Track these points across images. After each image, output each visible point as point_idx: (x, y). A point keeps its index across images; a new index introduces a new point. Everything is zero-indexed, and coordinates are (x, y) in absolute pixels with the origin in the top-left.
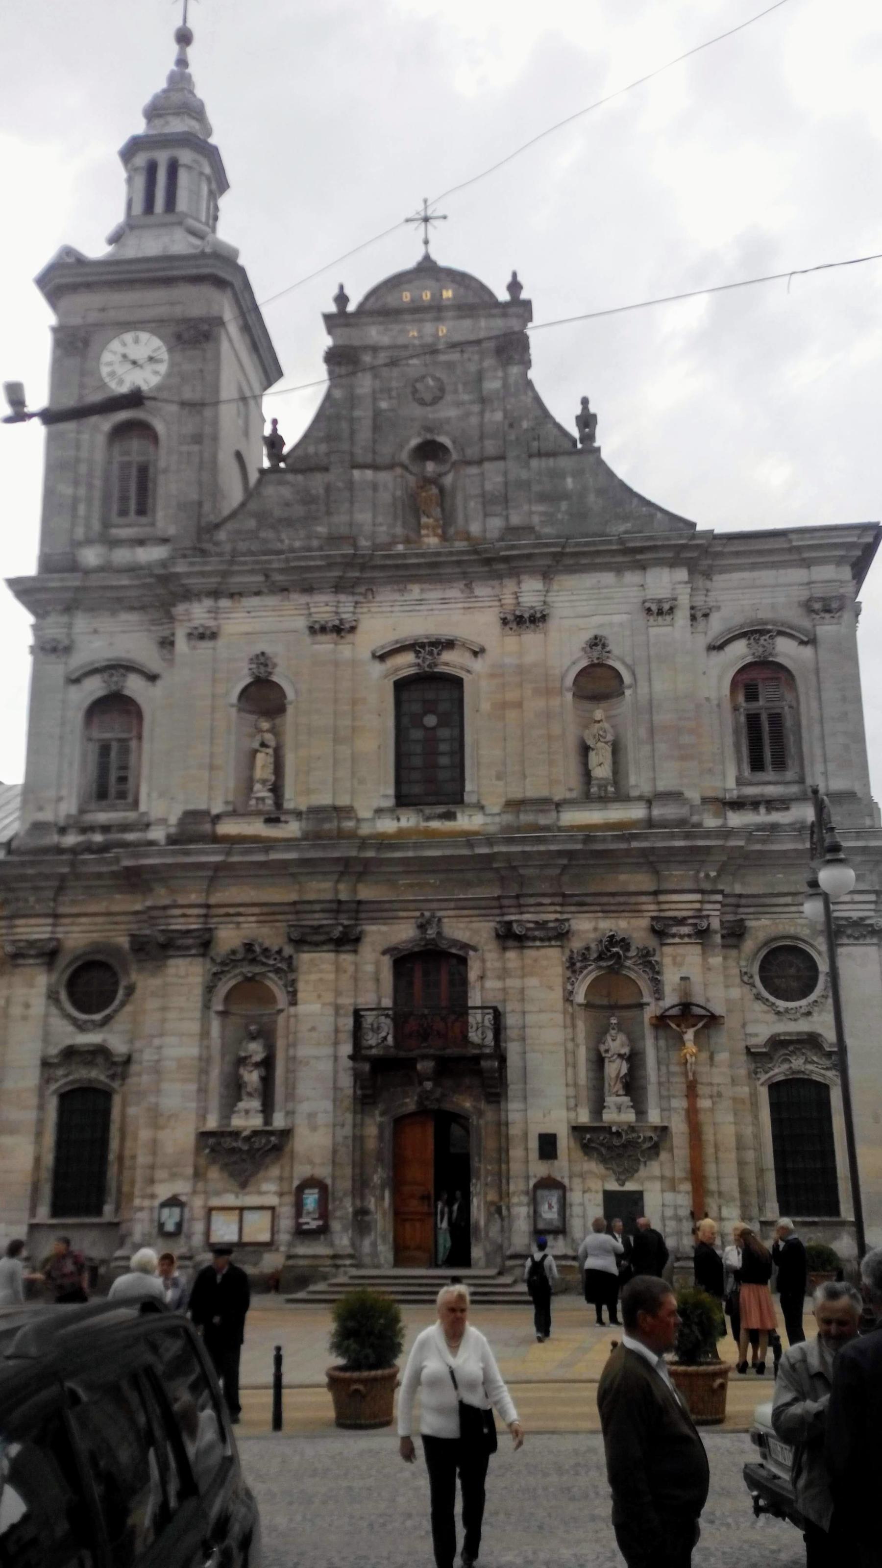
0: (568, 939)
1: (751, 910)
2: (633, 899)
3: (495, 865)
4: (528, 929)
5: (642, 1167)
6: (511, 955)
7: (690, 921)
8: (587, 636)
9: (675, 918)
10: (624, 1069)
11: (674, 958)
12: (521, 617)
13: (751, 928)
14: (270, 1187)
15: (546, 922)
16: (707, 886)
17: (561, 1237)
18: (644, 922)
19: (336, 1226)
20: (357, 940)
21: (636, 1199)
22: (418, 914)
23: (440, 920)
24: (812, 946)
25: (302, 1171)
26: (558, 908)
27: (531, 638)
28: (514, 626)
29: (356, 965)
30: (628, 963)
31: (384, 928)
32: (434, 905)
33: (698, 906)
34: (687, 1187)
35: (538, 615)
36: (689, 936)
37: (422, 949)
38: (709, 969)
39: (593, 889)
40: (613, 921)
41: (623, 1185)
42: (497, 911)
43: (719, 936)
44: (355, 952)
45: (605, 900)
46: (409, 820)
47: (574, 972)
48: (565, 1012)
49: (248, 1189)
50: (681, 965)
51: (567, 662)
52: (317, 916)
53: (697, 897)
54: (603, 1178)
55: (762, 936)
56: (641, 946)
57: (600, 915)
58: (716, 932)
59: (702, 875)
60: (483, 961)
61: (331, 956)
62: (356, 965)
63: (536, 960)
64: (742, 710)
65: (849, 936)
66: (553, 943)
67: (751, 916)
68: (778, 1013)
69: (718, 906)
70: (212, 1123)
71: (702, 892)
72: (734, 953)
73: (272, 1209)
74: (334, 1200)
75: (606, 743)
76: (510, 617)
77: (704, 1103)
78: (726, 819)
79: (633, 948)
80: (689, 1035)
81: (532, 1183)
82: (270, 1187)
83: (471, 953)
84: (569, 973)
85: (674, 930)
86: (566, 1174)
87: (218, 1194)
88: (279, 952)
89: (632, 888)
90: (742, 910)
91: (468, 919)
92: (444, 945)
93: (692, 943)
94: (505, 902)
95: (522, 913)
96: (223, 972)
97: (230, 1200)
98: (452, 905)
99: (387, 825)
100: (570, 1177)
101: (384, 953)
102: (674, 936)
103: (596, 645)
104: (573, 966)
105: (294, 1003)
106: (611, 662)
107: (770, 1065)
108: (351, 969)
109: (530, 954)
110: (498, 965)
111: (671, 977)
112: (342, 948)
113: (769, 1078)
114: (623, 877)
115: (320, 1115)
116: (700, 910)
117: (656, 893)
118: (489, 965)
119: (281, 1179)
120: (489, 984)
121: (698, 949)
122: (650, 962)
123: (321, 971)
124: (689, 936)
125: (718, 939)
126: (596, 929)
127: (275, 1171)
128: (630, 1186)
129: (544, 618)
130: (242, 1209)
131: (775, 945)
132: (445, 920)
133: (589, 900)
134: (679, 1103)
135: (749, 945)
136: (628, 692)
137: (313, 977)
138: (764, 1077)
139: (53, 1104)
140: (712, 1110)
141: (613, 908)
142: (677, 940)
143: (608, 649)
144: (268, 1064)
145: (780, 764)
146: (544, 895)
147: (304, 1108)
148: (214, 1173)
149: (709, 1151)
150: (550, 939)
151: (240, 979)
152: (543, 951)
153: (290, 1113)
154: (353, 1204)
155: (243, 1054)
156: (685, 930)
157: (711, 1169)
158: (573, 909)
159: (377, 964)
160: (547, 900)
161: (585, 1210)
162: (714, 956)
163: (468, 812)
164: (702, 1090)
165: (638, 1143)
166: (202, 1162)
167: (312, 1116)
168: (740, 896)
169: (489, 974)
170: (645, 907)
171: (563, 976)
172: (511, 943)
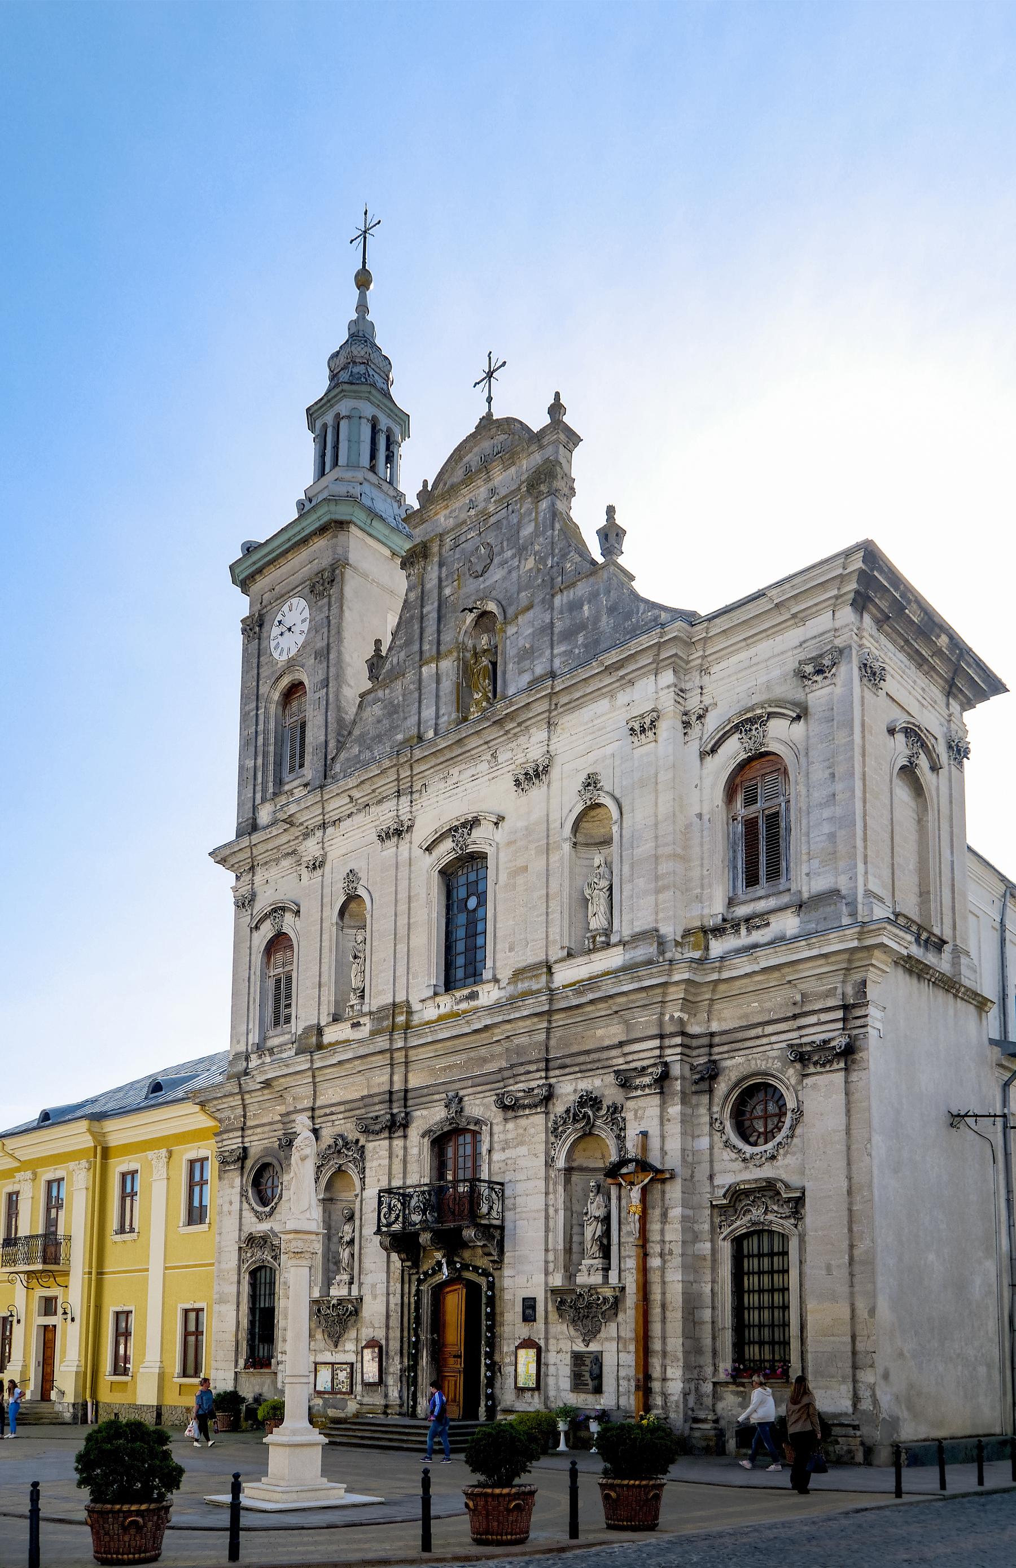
0: (554, 1104)
1: (725, 1048)
2: (605, 1055)
3: (495, 1039)
4: (517, 1099)
5: (603, 1328)
6: (510, 1125)
7: (650, 1070)
8: (582, 777)
9: (636, 1069)
10: (598, 1233)
11: (636, 1111)
12: (526, 774)
13: (724, 1069)
14: (350, 1346)
15: (533, 1089)
16: (669, 1029)
17: (536, 1393)
18: (611, 1079)
19: (391, 1380)
20: (405, 1126)
21: (597, 1359)
22: (444, 1096)
23: (461, 1100)
24: (781, 1080)
25: (367, 1333)
26: (543, 1074)
27: (537, 792)
28: (527, 787)
29: (405, 1148)
30: (599, 1122)
31: (425, 1112)
32: (458, 1085)
33: (657, 1052)
34: (632, 1348)
35: (541, 769)
36: (649, 1086)
37: (450, 1128)
38: (669, 1120)
39: (575, 1049)
40: (590, 1080)
41: (587, 1346)
42: (501, 1084)
43: (679, 1082)
44: (405, 1137)
45: (582, 1059)
46: (446, 1003)
47: (556, 1137)
48: (547, 1178)
49: (340, 1348)
50: (642, 1118)
51: (566, 811)
52: (377, 1108)
53: (656, 1043)
54: (572, 1339)
55: (734, 1076)
56: (610, 1103)
57: (579, 1075)
58: (676, 1079)
59: (667, 1017)
60: (491, 1134)
61: (387, 1142)
62: (405, 1148)
63: (525, 1129)
64: (739, 818)
65: (815, 1064)
66: (539, 1110)
67: (726, 1056)
68: (744, 1160)
69: (679, 1050)
70: (316, 1294)
71: (662, 1037)
72: (705, 1099)
73: (352, 1364)
74: (387, 1358)
75: (601, 890)
76: (521, 777)
77: (655, 1262)
78: (707, 948)
79: (605, 1107)
80: (636, 1194)
81: (517, 1344)
82: (350, 1346)
83: (484, 1128)
84: (552, 1139)
85: (638, 1081)
86: (542, 1336)
87: (321, 1351)
88: (357, 1141)
89: (607, 1043)
90: (716, 1050)
91: (482, 1095)
92: (463, 1124)
93: (646, 1095)
94: (506, 1074)
95: (517, 1083)
96: (323, 1165)
97: (328, 1357)
98: (470, 1083)
99: (431, 1013)
100: (547, 1339)
101: (423, 1136)
102: (636, 1088)
103: (589, 785)
104: (555, 1132)
105: (363, 1189)
106: (601, 800)
107: (733, 1218)
108: (401, 1153)
109: (523, 1122)
110: (502, 1137)
111: (632, 1133)
112: (396, 1135)
113: (732, 1232)
114: (599, 1032)
115: (378, 1286)
116: (660, 1057)
117: (621, 1044)
118: (496, 1138)
119: (357, 1340)
120: (496, 1156)
121: (656, 1100)
122: (616, 1118)
123: (380, 1158)
124: (649, 1086)
125: (678, 1086)
126: (575, 1091)
127: (352, 1334)
128: (593, 1347)
129: (546, 770)
130: (333, 1364)
131: (746, 1084)
132: (466, 1098)
133: (568, 1061)
134: (631, 1263)
135: (722, 1087)
136: (615, 828)
137: (375, 1164)
138: (726, 1231)
139: (246, 1277)
140: (663, 1269)
141: (589, 1066)
142: (639, 1092)
143: (599, 786)
144: (351, 1242)
145: (774, 873)
146: (530, 1062)
147: (368, 1280)
148: (319, 1336)
149: (656, 1311)
150: (536, 1106)
151: (333, 1170)
152: (532, 1119)
153: (360, 1284)
154: (401, 1362)
155: (340, 1234)
156: (647, 1080)
157: (656, 1328)
158: (557, 1072)
159: (420, 1146)
160: (533, 1067)
161: (558, 1369)
162: (674, 1105)
163: (485, 986)
164: (655, 1248)
165: (598, 1305)
166: (313, 1326)
167: (374, 1286)
168: (712, 1035)
169: (496, 1146)
170: (615, 1062)
171: (547, 1142)
172: (510, 1114)
